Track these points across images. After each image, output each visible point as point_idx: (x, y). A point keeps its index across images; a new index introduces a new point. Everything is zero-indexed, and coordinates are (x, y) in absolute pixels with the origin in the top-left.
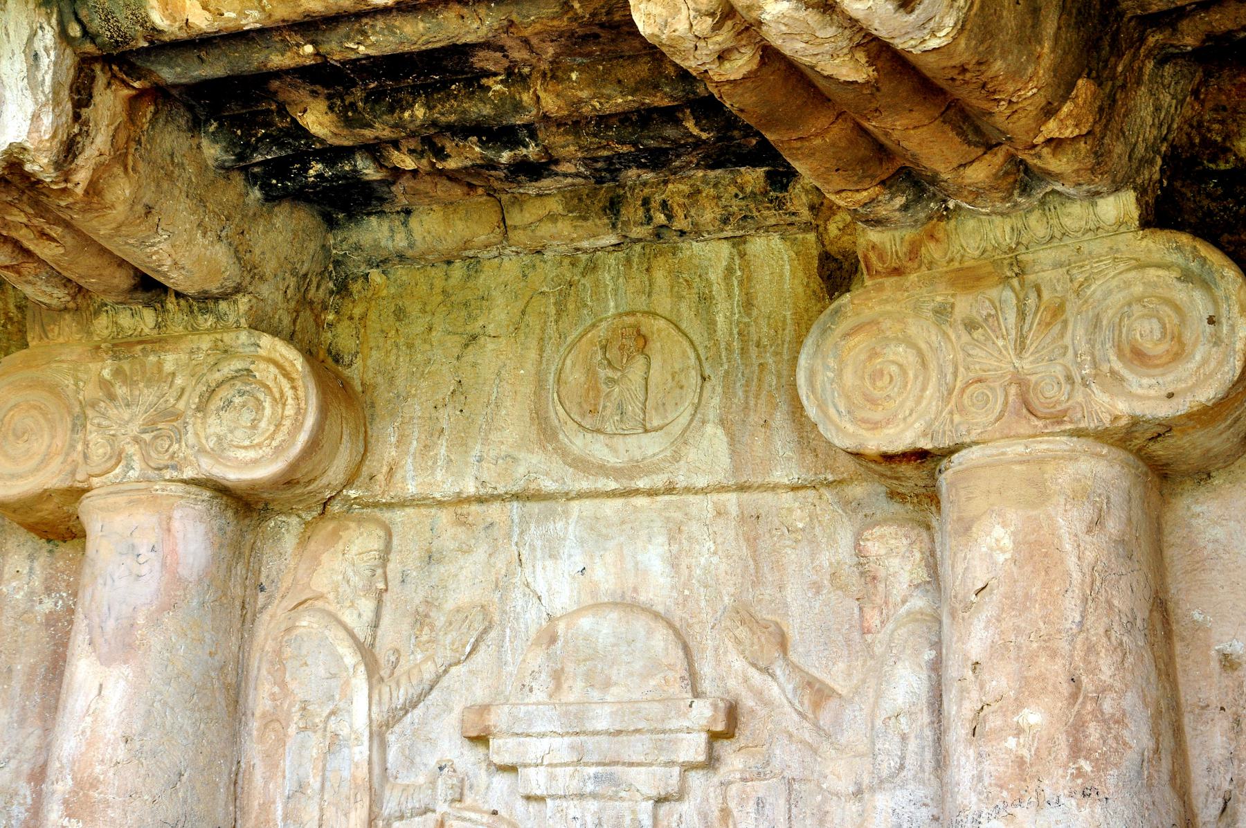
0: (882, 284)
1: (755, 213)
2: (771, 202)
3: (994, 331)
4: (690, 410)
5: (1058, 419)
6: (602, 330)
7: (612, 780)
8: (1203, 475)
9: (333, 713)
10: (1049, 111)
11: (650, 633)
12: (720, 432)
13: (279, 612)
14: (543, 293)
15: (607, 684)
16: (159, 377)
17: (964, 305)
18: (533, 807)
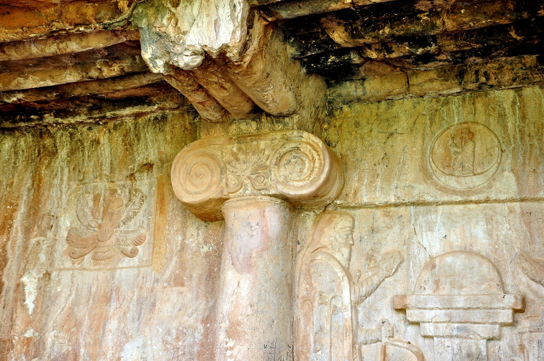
2: (539, 70)
4: (496, 165)
6: (452, 130)
9: (334, 297)
11: (480, 264)
12: (511, 175)
13: (307, 253)
14: (423, 114)
15: (461, 287)
16: (257, 151)
18: (427, 341)
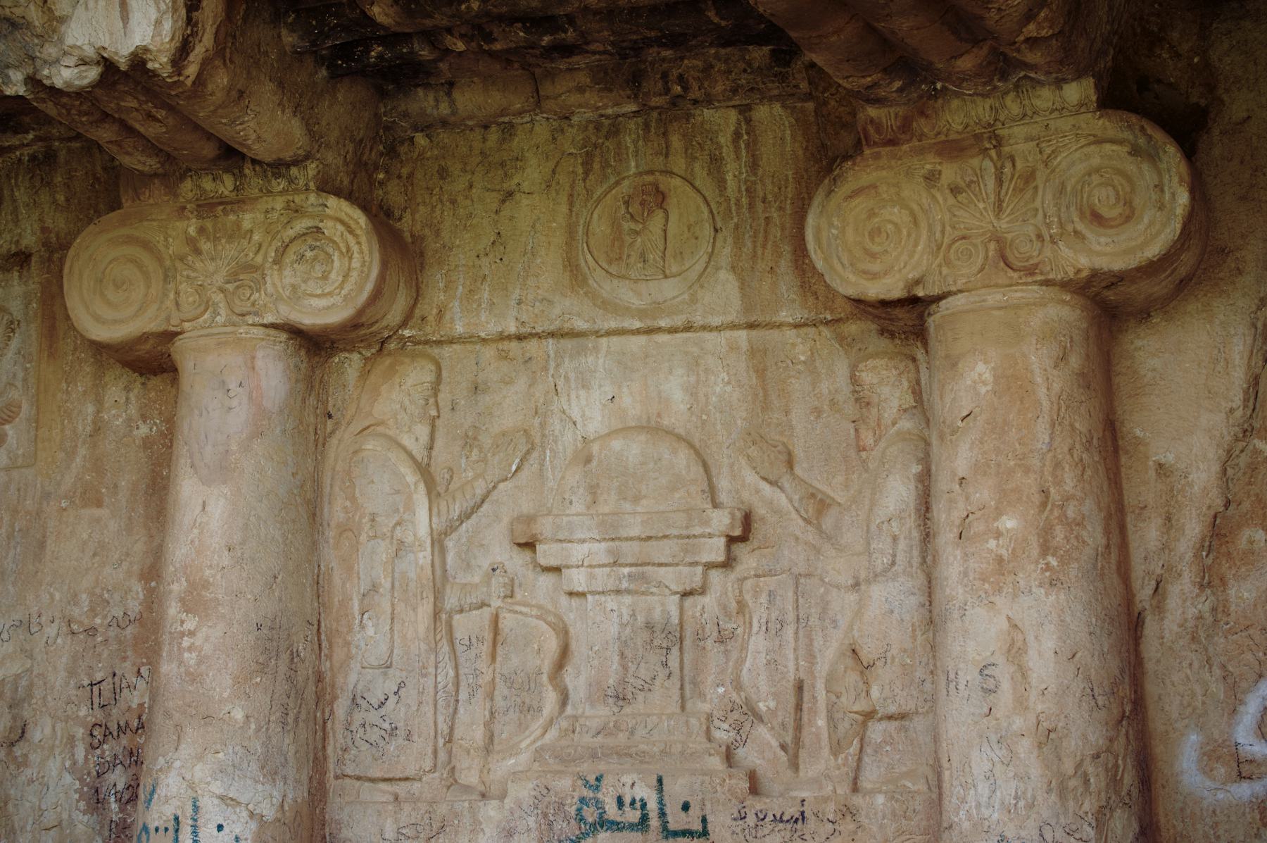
0: (878, 153)
1: (761, 86)
2: (775, 76)
3: (976, 195)
4: (705, 258)
5: (1031, 271)
7: (643, 578)
8: (1144, 314)
9: (398, 523)
10: (1029, 17)
12: (731, 277)
15: (637, 499)
16: (236, 233)
17: (950, 172)
18: (575, 602)
